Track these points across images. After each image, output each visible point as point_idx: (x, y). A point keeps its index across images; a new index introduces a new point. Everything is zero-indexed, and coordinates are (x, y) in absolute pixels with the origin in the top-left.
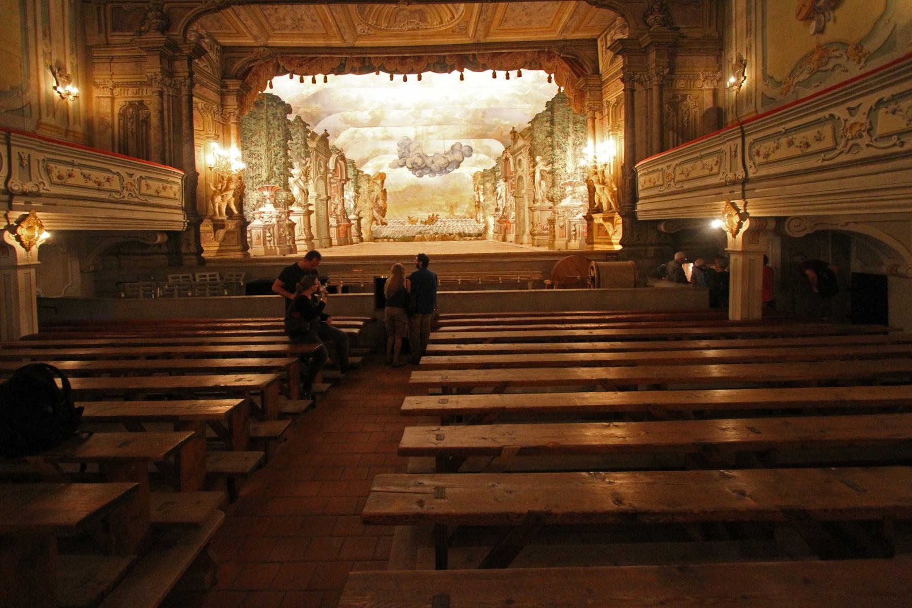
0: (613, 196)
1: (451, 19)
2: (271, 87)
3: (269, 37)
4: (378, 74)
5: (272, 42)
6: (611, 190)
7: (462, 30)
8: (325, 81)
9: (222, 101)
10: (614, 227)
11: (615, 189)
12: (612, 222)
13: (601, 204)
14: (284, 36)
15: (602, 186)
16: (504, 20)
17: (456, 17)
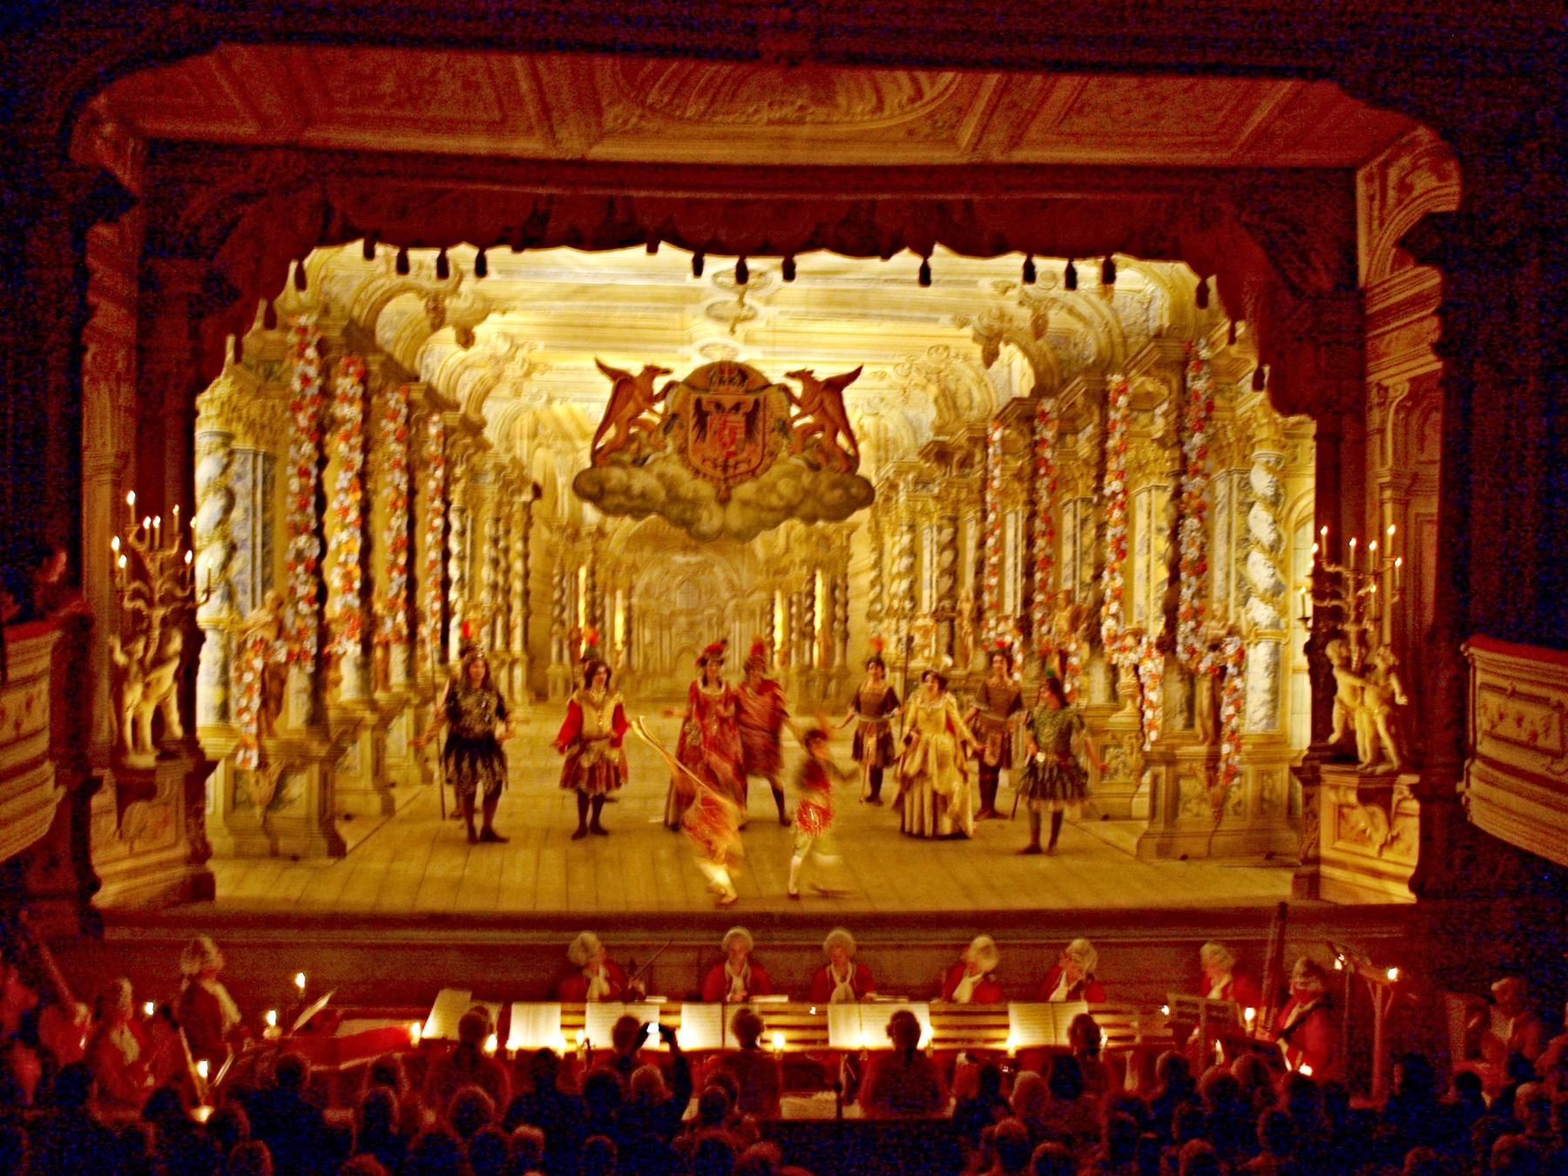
0: (1389, 721)
1: (912, 100)
2: (301, 283)
3: (309, 122)
4: (652, 249)
5: (311, 135)
6: (1389, 700)
7: (942, 128)
8: (481, 269)
9: (142, 333)
10: (1390, 824)
11: (1401, 700)
12: (1387, 807)
13: (1349, 734)
14: (358, 122)
15: (1358, 683)
16: (1076, 108)
17: (928, 96)
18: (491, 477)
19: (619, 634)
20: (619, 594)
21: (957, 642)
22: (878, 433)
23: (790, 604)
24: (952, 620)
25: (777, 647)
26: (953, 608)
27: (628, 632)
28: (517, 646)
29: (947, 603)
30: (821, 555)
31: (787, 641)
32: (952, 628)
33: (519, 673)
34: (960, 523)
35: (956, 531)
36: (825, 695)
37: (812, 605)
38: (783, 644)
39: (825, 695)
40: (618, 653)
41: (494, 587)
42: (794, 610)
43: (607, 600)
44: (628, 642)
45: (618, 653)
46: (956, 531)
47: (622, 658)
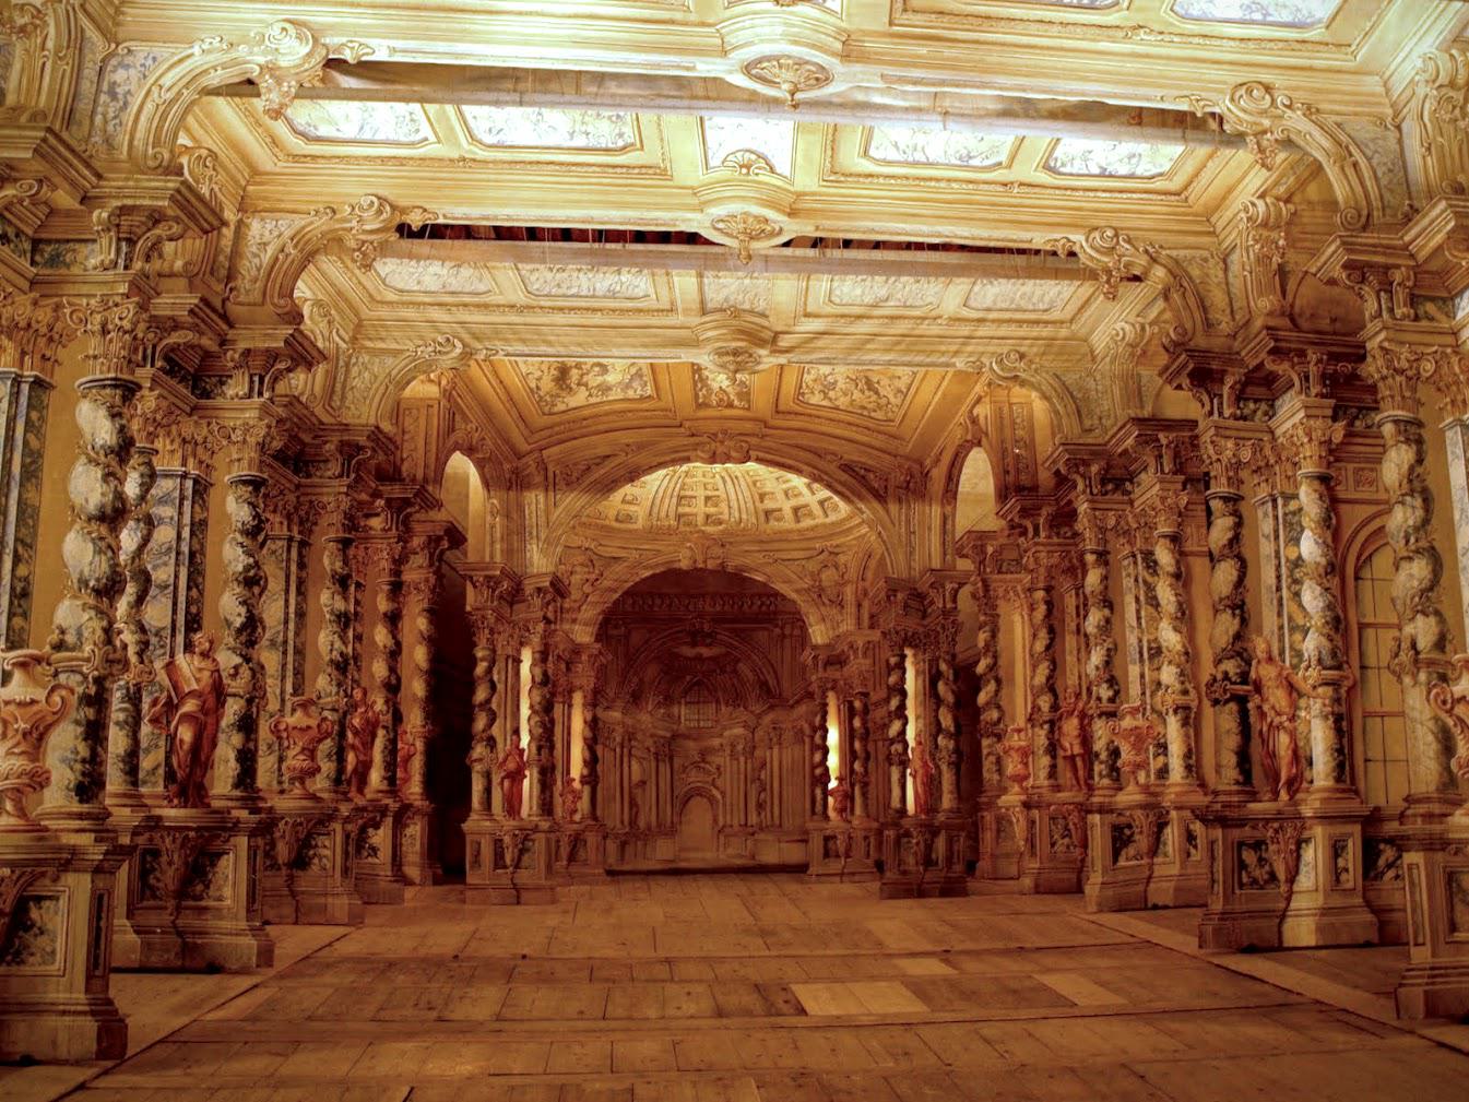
18: (334, 468)
19: (577, 769)
20: (578, 698)
21: (1256, 742)
22: (1001, 428)
23: (852, 713)
24: (1242, 701)
25: (833, 784)
26: (1244, 677)
27: (592, 762)
28: (414, 789)
29: (1230, 667)
30: (912, 624)
31: (847, 775)
32: (1244, 715)
33: (415, 831)
34: (1244, 507)
35: (1239, 525)
36: (928, 861)
37: (902, 707)
38: (840, 779)
39: (928, 861)
40: (577, 796)
41: (342, 666)
42: (857, 723)
43: (558, 710)
44: (591, 778)
45: (577, 796)
46: (1239, 525)
47: (584, 805)
